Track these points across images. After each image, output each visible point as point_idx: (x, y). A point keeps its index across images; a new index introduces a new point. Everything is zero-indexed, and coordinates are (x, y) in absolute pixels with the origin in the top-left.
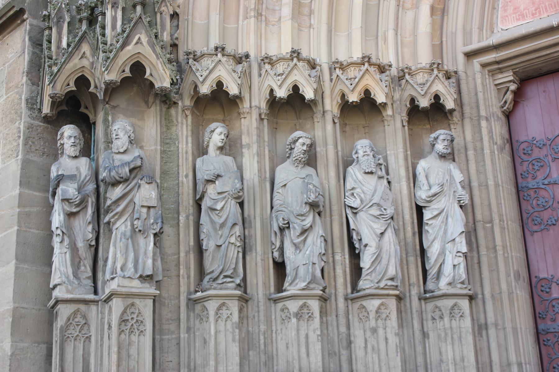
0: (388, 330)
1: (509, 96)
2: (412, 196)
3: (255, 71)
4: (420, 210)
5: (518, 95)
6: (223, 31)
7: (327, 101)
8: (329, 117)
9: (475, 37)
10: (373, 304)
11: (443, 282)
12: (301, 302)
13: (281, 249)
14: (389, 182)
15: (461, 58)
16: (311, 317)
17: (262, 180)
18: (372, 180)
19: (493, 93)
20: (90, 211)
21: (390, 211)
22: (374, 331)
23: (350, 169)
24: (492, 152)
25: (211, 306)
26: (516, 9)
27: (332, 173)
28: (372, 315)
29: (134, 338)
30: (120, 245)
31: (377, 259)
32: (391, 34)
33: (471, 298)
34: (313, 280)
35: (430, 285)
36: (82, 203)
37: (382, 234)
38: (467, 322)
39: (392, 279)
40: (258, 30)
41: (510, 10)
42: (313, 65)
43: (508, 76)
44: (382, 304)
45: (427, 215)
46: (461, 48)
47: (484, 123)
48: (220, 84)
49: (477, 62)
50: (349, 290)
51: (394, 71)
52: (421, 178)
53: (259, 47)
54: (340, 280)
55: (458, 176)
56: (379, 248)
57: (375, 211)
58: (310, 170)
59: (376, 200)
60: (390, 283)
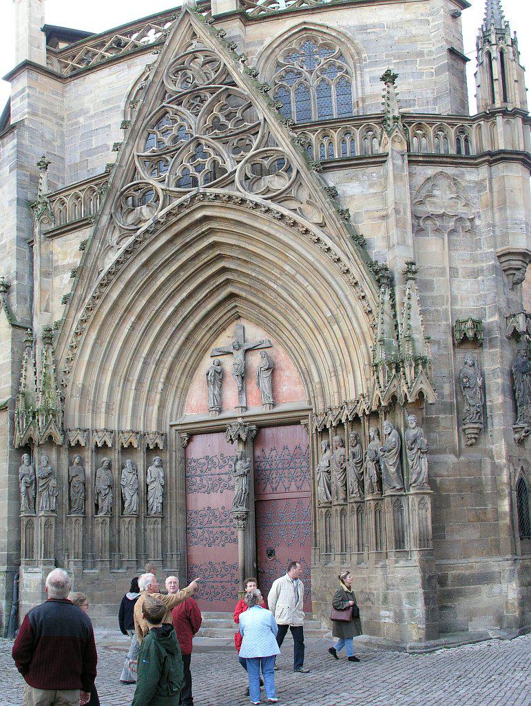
1: (185, 442)
3: (91, 435)
4: (147, 485)
5: (189, 441)
6: (80, 420)
7: (117, 445)
9: (174, 419)
11: (153, 512)
15: (168, 427)
17: (92, 474)
19: (178, 440)
20: (33, 485)
21: (136, 487)
25: (74, 519)
27: (117, 472)
29: (49, 530)
30: (45, 499)
31: (130, 504)
32: (142, 417)
33: (162, 518)
36: (31, 483)
38: (160, 526)
40: (92, 417)
43: (185, 435)
46: (169, 423)
48: (78, 441)
49: (174, 428)
51: (142, 433)
53: (92, 425)
54: (117, 510)
56: (131, 501)
58: (109, 471)
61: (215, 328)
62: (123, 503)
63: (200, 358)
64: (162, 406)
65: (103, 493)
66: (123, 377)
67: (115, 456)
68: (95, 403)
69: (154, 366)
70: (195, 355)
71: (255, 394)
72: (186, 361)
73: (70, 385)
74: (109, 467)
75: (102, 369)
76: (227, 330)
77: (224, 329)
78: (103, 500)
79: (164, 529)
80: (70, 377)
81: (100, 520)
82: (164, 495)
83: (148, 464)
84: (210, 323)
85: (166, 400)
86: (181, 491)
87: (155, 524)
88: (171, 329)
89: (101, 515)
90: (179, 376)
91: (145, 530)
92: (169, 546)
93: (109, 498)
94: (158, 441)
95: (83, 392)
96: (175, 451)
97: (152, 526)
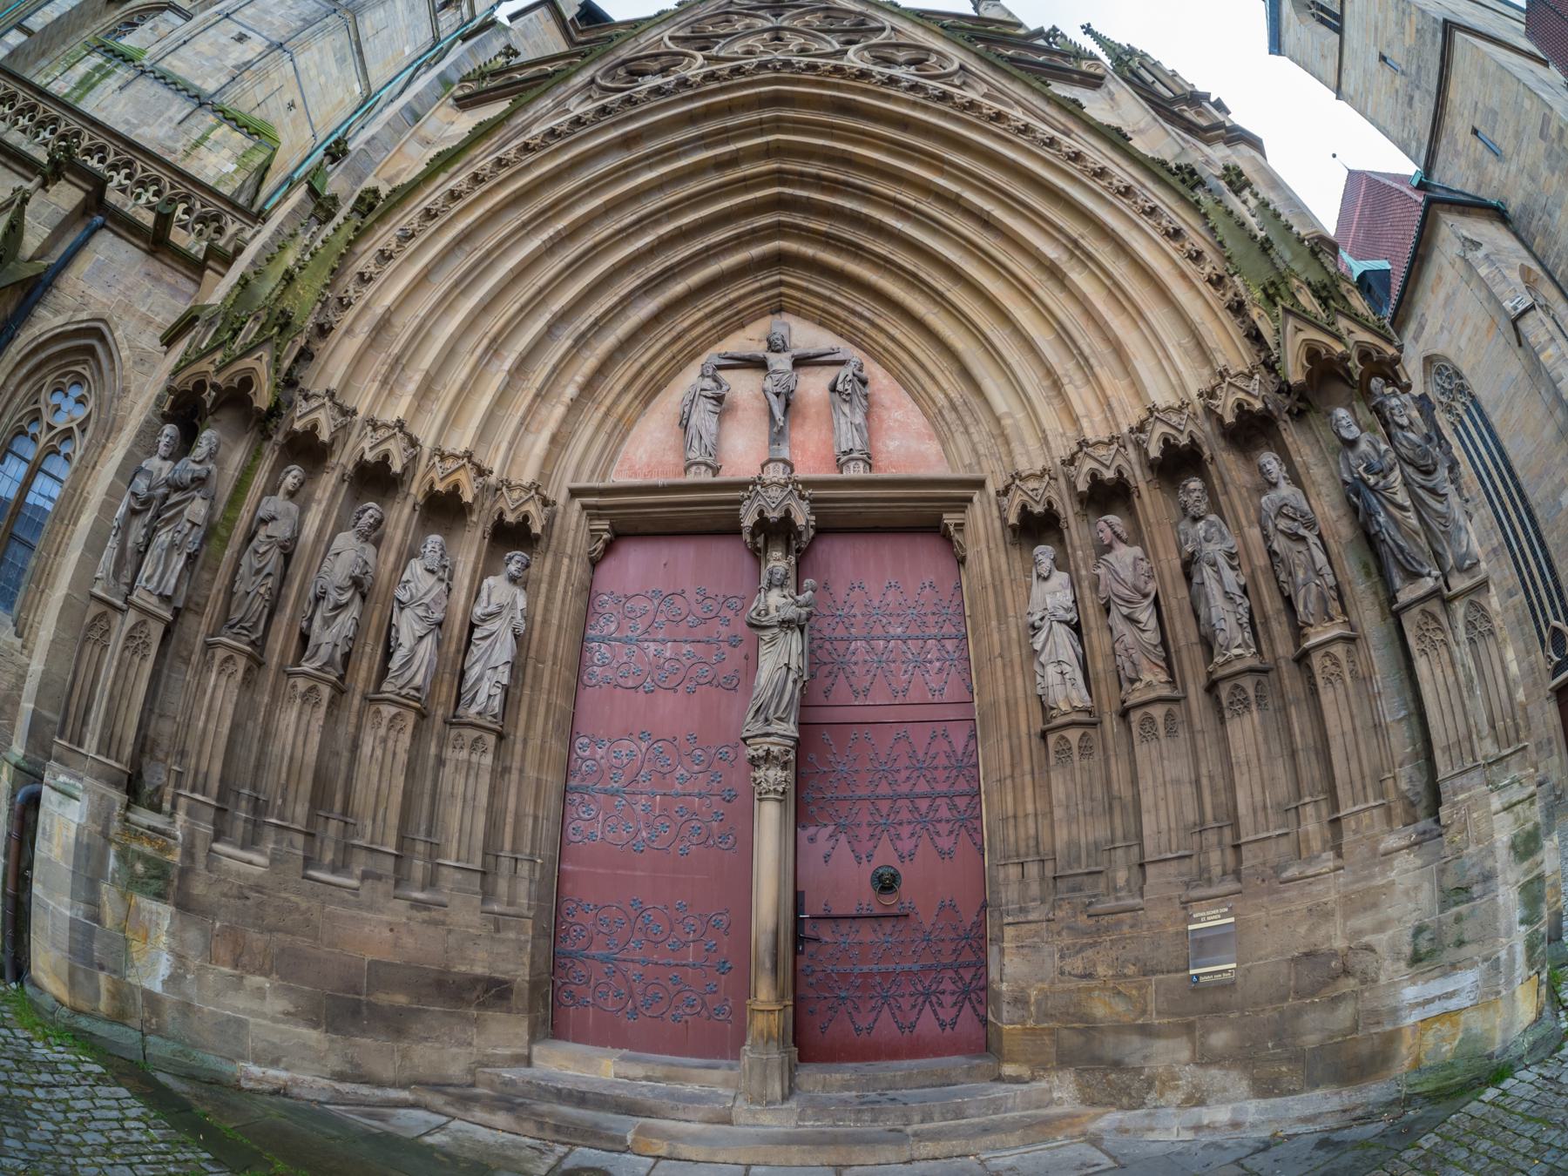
0: (399, 744)
1: (600, 545)
2: (468, 610)
4: (472, 627)
5: (609, 548)
7: (415, 485)
8: (410, 502)
10: (388, 711)
11: (474, 710)
12: (311, 683)
13: (311, 620)
14: (450, 590)
15: (564, 493)
16: (317, 704)
18: (432, 579)
19: (583, 535)
21: (438, 616)
22: (384, 740)
23: (413, 561)
24: (565, 592)
26: (631, 467)
27: (392, 558)
28: (385, 722)
31: (408, 663)
32: (504, 446)
34: (330, 662)
35: (461, 711)
37: (421, 638)
38: (488, 760)
39: (417, 689)
41: (626, 466)
42: (413, 442)
43: (604, 525)
44: (399, 714)
45: (477, 634)
46: (568, 483)
47: (566, 561)
49: (577, 503)
50: (371, 689)
51: (493, 479)
52: (484, 594)
54: (363, 674)
55: (521, 602)
57: (421, 612)
58: (370, 549)
59: (426, 600)
60: (413, 692)
61: (726, 313)
62: (388, 655)
63: (676, 367)
64: (558, 442)
65: (333, 596)
66: (491, 335)
67: (401, 515)
68: (398, 364)
69: (569, 342)
70: (668, 354)
72: (644, 359)
73: (360, 304)
74: (375, 535)
75: (446, 304)
77: (742, 326)
78: (327, 622)
79: (500, 772)
80: (369, 291)
81: (302, 685)
82: (517, 667)
83: (488, 567)
84: (716, 300)
85: (572, 434)
86: (566, 673)
87: (473, 748)
88: (629, 283)
89: (307, 667)
90: (618, 388)
91: (440, 762)
92: (509, 830)
93: (345, 621)
94: (532, 508)
95: (383, 325)
96: (571, 558)
97: (464, 754)
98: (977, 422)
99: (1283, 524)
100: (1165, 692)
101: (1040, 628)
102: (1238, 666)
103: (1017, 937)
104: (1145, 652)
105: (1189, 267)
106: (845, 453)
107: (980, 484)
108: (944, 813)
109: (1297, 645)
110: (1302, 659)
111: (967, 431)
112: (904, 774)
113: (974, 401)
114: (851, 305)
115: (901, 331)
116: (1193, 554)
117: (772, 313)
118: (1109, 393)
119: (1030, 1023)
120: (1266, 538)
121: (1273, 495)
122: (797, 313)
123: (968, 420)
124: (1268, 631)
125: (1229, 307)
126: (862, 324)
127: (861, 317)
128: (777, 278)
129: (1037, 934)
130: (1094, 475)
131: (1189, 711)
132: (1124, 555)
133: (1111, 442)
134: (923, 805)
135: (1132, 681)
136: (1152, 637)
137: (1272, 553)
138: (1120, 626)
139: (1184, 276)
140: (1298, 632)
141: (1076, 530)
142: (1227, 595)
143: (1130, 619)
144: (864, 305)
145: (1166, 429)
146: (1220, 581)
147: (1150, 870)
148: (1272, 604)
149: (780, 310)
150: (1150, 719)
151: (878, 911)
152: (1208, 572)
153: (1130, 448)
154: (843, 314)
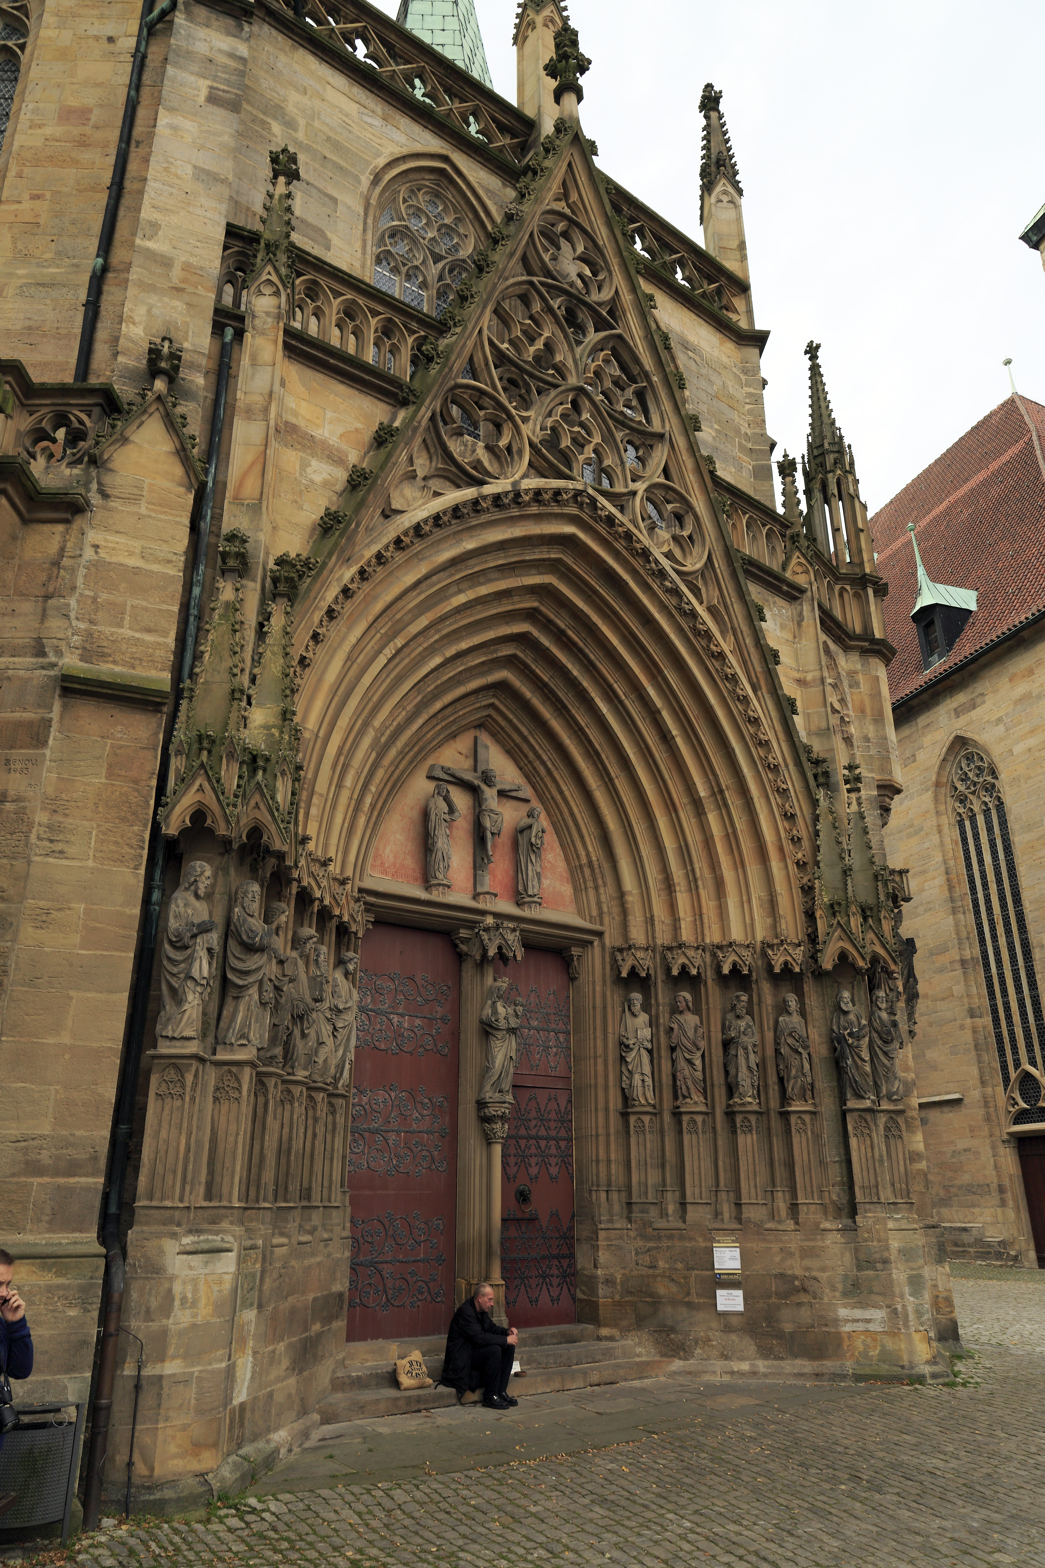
26: (382, 864)
41: (378, 863)
71: (500, 877)
76: (458, 739)
98: (605, 885)
99: (790, 1041)
100: (703, 1108)
101: (632, 1049)
102: (749, 1108)
103: (608, 1239)
104: (694, 1082)
105: (788, 847)
106: (530, 896)
107: (600, 934)
108: (553, 1151)
109: (782, 1105)
110: (785, 1116)
111: (596, 888)
112: (534, 1122)
113: (606, 866)
114: (540, 751)
115: (569, 789)
116: (733, 1038)
117: (475, 727)
118: (704, 911)
119: (617, 1297)
120: (777, 1043)
121: (787, 1019)
122: (494, 735)
123: (600, 882)
124: (767, 1094)
125: (802, 888)
126: (542, 770)
127: (543, 763)
128: (492, 701)
129: (621, 1238)
130: (684, 966)
131: (714, 1122)
132: (690, 1020)
133: (697, 948)
134: (543, 1143)
135: (684, 1097)
136: (699, 1075)
137: (777, 1051)
138: (682, 1064)
139: (781, 849)
140: (784, 1099)
141: (661, 994)
142: (749, 1067)
143: (690, 1062)
144: (547, 754)
145: (737, 959)
146: (747, 1059)
147: (689, 1208)
148: (772, 1079)
149: (480, 726)
150: (695, 1122)
151: (519, 1215)
152: (741, 1052)
153: (708, 954)
154: (531, 756)
